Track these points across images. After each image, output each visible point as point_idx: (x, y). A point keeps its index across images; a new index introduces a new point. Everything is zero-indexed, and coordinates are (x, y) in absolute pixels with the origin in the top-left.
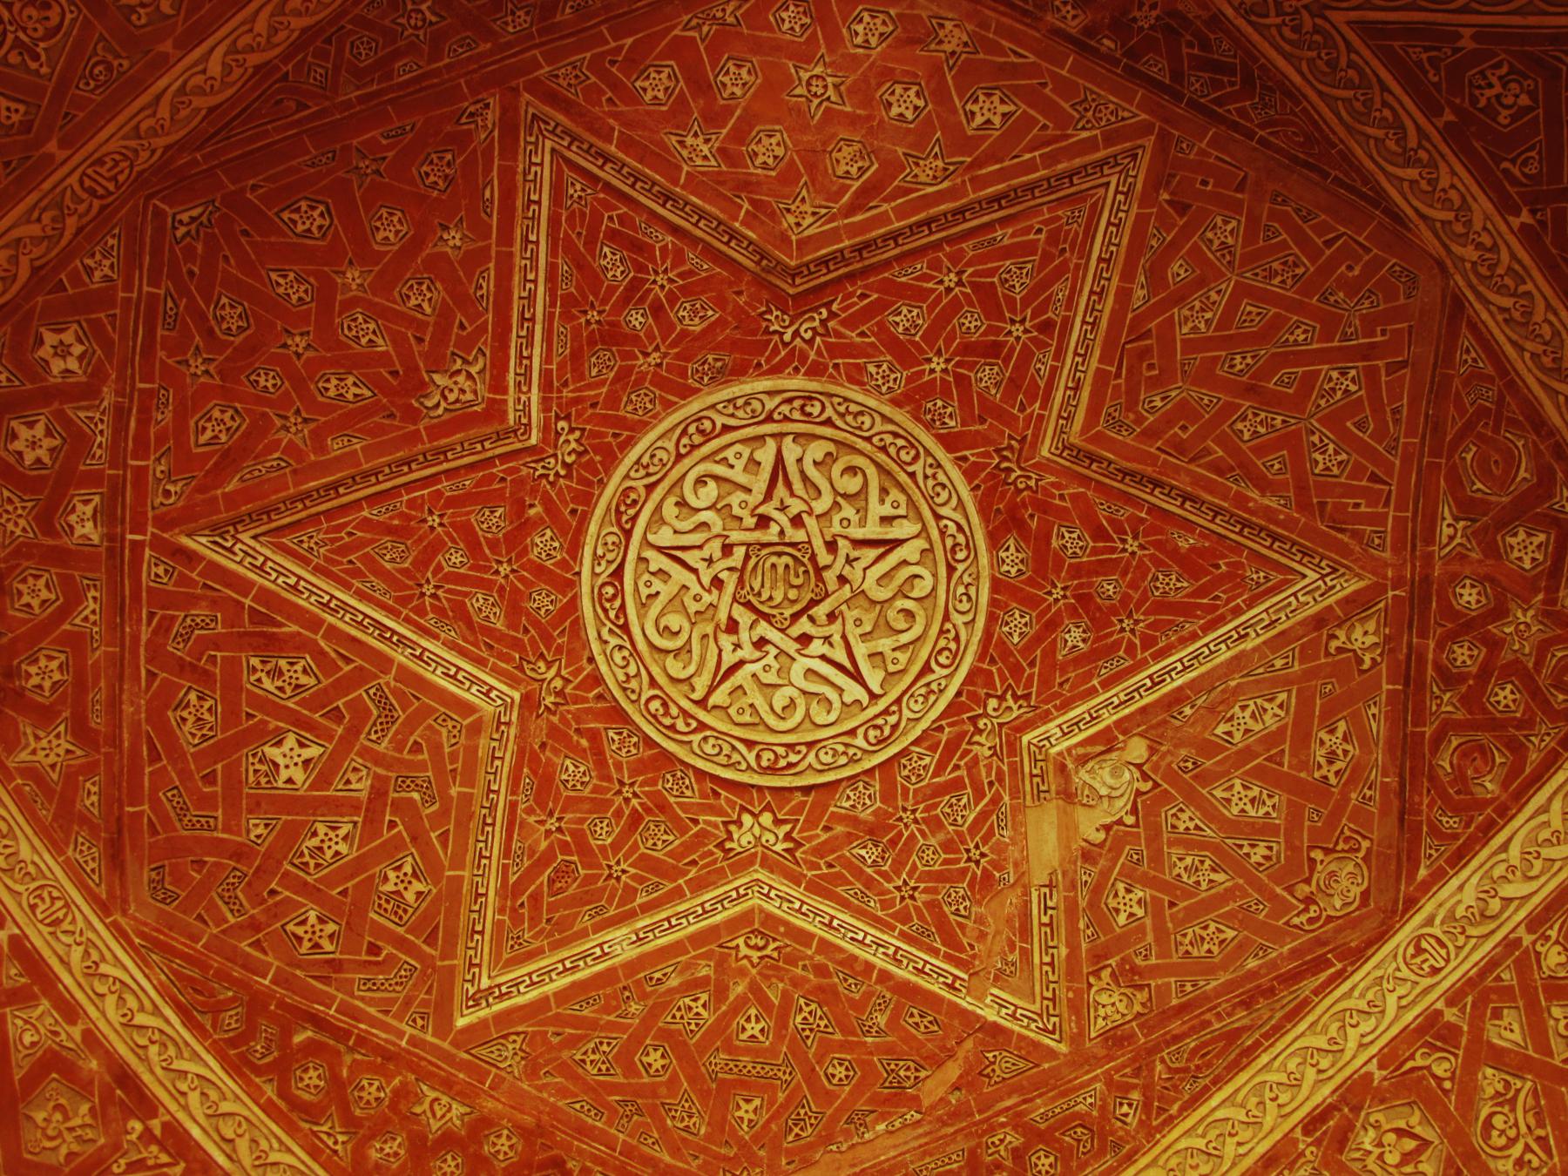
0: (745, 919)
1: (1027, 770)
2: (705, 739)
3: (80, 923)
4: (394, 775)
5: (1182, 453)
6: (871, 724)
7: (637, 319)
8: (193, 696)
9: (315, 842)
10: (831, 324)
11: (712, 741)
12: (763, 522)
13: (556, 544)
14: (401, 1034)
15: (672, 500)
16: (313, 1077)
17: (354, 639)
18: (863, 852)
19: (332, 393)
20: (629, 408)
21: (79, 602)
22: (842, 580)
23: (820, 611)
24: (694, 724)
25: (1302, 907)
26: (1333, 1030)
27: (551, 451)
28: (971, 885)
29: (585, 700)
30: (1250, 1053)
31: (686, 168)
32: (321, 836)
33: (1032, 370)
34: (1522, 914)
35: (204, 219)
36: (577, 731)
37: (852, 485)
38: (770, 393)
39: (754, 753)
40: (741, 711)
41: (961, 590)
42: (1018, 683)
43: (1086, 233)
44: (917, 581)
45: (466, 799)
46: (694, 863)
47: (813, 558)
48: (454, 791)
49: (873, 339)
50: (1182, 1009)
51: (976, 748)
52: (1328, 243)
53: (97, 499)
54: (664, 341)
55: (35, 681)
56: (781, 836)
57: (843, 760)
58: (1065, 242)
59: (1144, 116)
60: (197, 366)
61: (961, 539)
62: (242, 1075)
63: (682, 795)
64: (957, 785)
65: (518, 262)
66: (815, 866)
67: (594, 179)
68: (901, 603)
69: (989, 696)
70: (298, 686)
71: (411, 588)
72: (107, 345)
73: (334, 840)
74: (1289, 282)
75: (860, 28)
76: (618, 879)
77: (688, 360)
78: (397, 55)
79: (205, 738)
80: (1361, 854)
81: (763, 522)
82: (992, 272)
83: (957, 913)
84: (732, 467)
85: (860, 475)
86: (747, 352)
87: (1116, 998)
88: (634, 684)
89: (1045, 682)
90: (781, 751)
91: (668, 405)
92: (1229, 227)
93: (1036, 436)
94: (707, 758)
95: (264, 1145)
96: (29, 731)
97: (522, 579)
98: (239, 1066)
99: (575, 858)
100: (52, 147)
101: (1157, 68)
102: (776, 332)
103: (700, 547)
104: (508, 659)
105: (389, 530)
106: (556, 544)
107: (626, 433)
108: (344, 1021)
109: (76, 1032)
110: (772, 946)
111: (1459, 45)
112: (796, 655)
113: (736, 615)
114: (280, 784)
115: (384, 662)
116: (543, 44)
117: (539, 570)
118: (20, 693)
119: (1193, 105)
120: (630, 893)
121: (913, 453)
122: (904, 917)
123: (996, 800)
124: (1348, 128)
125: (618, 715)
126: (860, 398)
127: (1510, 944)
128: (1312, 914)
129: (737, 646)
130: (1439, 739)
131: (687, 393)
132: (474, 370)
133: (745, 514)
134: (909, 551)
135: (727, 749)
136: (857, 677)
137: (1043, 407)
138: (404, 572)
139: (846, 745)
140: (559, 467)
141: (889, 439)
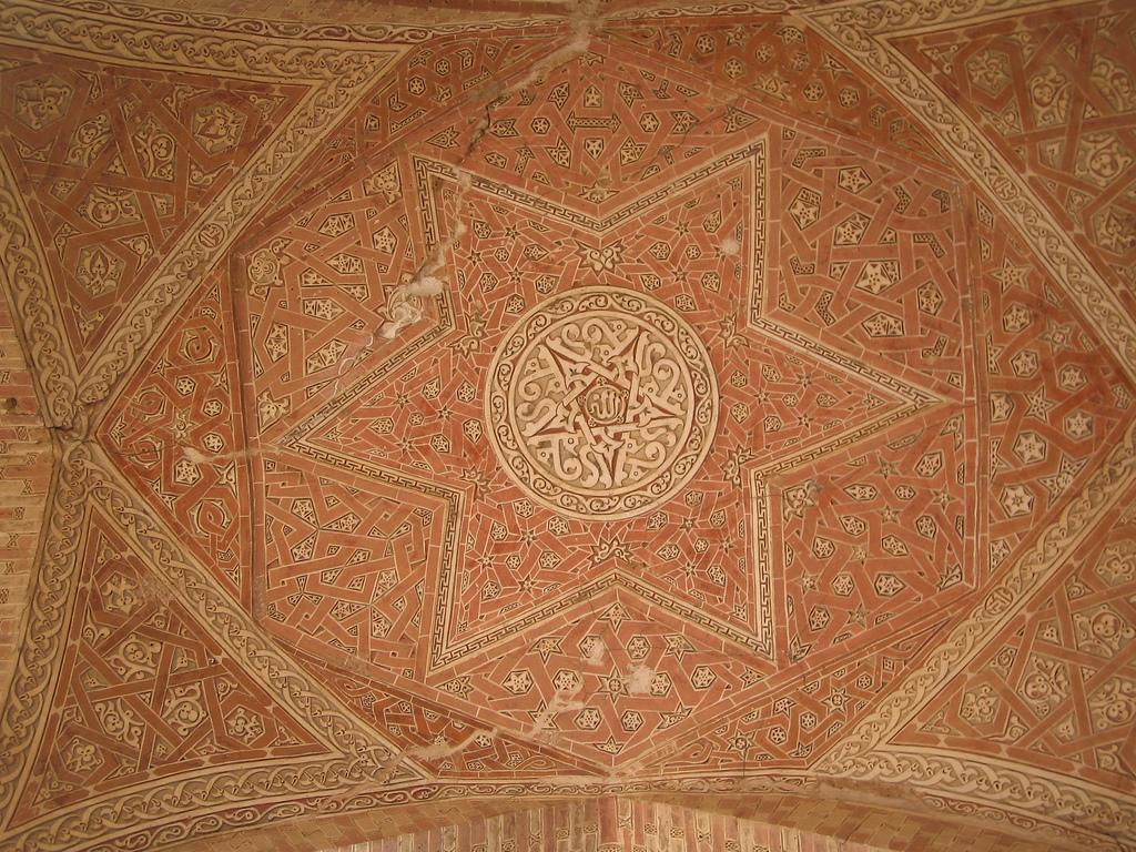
0: (605, 209)
2: (638, 309)
3: (986, 180)
4: (816, 274)
5: (386, 503)
7: (701, 545)
8: (933, 311)
9: (858, 232)
10: (592, 553)
11: (635, 308)
12: (617, 437)
14: (799, 126)
16: (848, 99)
17: (844, 350)
19: (868, 489)
20: (700, 495)
21: (1001, 360)
22: (568, 408)
23: (579, 388)
25: (284, 251)
26: (260, 185)
28: (475, 241)
29: (710, 326)
30: (305, 166)
31: (683, 633)
32: (854, 236)
34: (161, 268)
35: (945, 581)
36: (711, 307)
37: (569, 463)
38: (621, 511)
39: (609, 304)
41: (500, 410)
42: (461, 360)
45: (773, 263)
48: (780, 268)
50: (346, 184)
52: (321, 629)
53: (994, 419)
55: (1021, 314)
56: (588, 257)
59: (433, 688)
60: (943, 498)
62: (888, 98)
64: (489, 298)
65: (771, 573)
66: (569, 242)
67: (731, 622)
68: (535, 397)
69: (477, 350)
70: (874, 320)
71: (815, 381)
72: (993, 505)
73: (846, 234)
74: (339, 605)
75: (595, 719)
78: (847, 679)
79: (924, 287)
80: (253, 287)
82: (505, 592)
84: (639, 467)
86: (639, 535)
87: (385, 185)
88: (683, 338)
89: (446, 362)
90: (594, 307)
91: (678, 497)
92: (377, 631)
93: (469, 502)
94: (637, 299)
95: (872, 61)
96: (1023, 286)
97: (752, 392)
98: (888, 103)
99: (707, 234)
100: (1029, 616)
101: (430, 716)
102: (623, 545)
103: (652, 419)
104: (755, 345)
105: (829, 412)
106: (734, 414)
108: (832, 131)
109: (984, 121)
110: (588, 195)
111: (272, 748)
113: (628, 382)
114: (879, 264)
115: (826, 337)
116: (767, 694)
117: (742, 397)
118: (1029, 306)
119: (407, 697)
120: (673, 217)
121: (537, 485)
122: (512, 218)
123: (466, 292)
124: (321, 695)
125: (687, 319)
126: (570, 514)
127: (166, 250)
128: (277, 248)
129: (625, 364)
130: (221, 357)
131: (669, 506)
132: (790, 509)
133: (628, 441)
134: (531, 429)
138: (818, 390)
141: (551, 492)
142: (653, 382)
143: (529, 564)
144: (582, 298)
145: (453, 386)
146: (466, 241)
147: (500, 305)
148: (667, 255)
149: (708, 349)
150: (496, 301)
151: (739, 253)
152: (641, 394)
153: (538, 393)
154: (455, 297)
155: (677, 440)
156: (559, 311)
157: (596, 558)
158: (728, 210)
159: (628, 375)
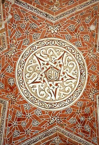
0: (56, 14)
1: (6, 43)
6: (35, 50)
11: (63, 45)
12: (57, 85)
13: (92, 78)
15: (73, 87)
18: (35, 26)
22: (42, 75)
23: (45, 69)
24: (66, 48)
27: (94, 94)
29: (85, 51)
33: (11, 117)
37: (42, 92)
39: (55, 44)
40: (58, 51)
43: (4, 144)
44: (28, 76)
46: (65, 23)
47: (47, 79)
49: (41, 119)
51: (15, 46)
54: (77, 116)
56: (50, 29)
57: (39, 43)
58: (8, 141)
61: (21, 84)
63: (68, 35)
64: (18, 39)
66: (44, 23)
76: (78, 20)
77: (73, 112)
81: (57, 85)
82: (21, 134)
83: (17, 15)
85: (41, 94)
86: (63, 115)
90: (51, 44)
94: (64, 42)
99: (86, 23)
102: (58, 119)
103: (67, 79)
107: (82, 99)
110: (51, 9)
112: (49, 61)
113: (60, 68)
117: (94, 73)
120: (76, 17)
123: (11, 37)
125: (80, 49)
129: (59, 62)
131: (72, 106)
133: (60, 86)
134: (30, 81)
135: (60, 44)
136: (38, 58)
137: (8, 110)
139: (39, 46)
140: (92, 92)
141: (36, 101)
142: (68, 68)
143: (29, 124)
144: (47, 41)
145: (5, 67)
146: (12, 21)
147: (22, 42)
148: (74, 29)
149: (85, 58)
150: (20, 41)
151: (95, 30)
152: (64, 72)
153: (32, 70)
154: (7, 38)
155: (75, 86)
156: (40, 45)
157: (50, 123)
158: (93, 16)
159: (60, 65)
